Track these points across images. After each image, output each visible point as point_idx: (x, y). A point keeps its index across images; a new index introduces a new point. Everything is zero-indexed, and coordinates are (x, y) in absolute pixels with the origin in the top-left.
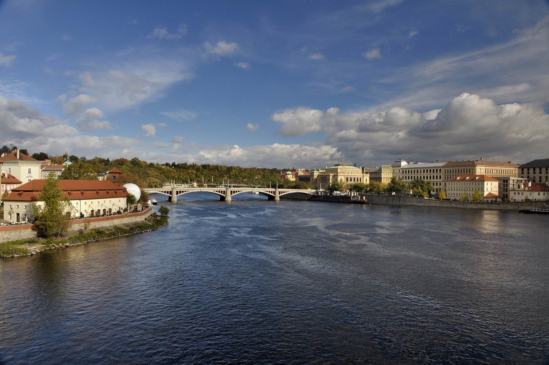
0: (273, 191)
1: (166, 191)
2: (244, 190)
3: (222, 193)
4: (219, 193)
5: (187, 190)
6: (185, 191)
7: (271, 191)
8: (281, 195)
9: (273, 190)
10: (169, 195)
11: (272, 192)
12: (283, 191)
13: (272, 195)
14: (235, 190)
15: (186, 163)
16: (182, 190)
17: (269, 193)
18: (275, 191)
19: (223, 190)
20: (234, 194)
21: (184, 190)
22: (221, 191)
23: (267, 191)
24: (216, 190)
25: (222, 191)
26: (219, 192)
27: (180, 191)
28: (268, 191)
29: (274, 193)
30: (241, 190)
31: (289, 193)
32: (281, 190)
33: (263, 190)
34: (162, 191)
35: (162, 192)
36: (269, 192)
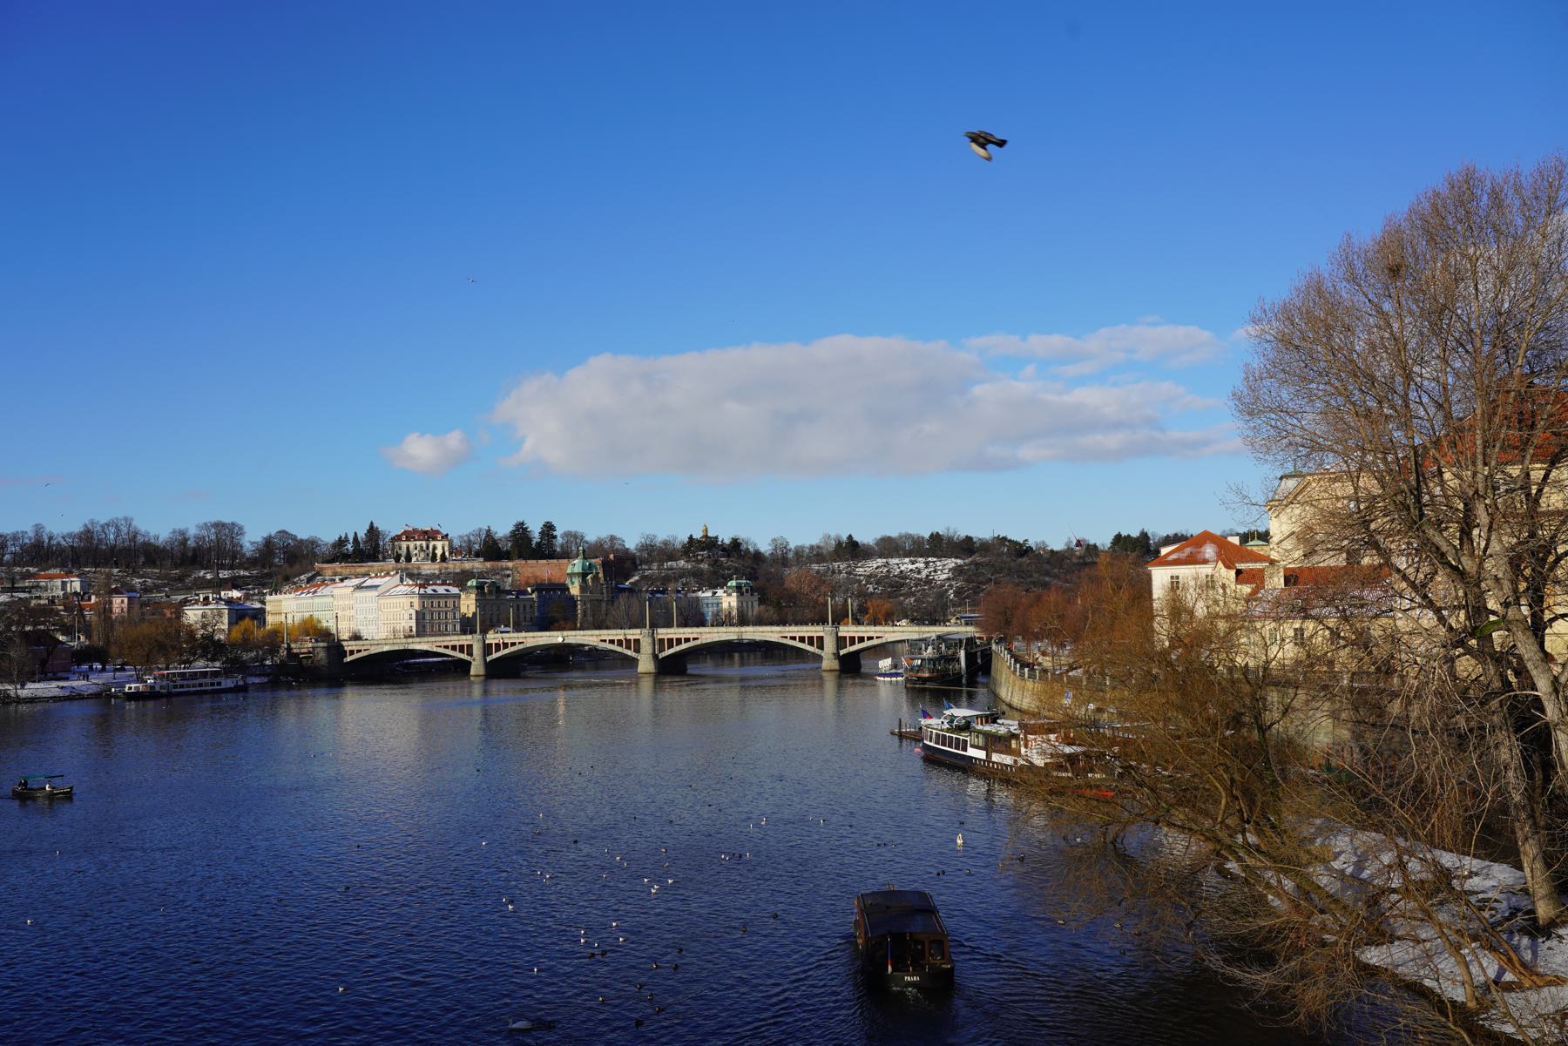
0: (815, 635)
1: (804, 637)
3: (628, 647)
4: (619, 649)
5: (517, 641)
7: (806, 635)
12: (856, 635)
14: (675, 637)
17: (800, 645)
19: (632, 638)
20: (672, 651)
22: (626, 639)
25: (628, 641)
28: (797, 635)
30: (695, 636)
32: (848, 630)
34: (446, 644)
35: (446, 647)
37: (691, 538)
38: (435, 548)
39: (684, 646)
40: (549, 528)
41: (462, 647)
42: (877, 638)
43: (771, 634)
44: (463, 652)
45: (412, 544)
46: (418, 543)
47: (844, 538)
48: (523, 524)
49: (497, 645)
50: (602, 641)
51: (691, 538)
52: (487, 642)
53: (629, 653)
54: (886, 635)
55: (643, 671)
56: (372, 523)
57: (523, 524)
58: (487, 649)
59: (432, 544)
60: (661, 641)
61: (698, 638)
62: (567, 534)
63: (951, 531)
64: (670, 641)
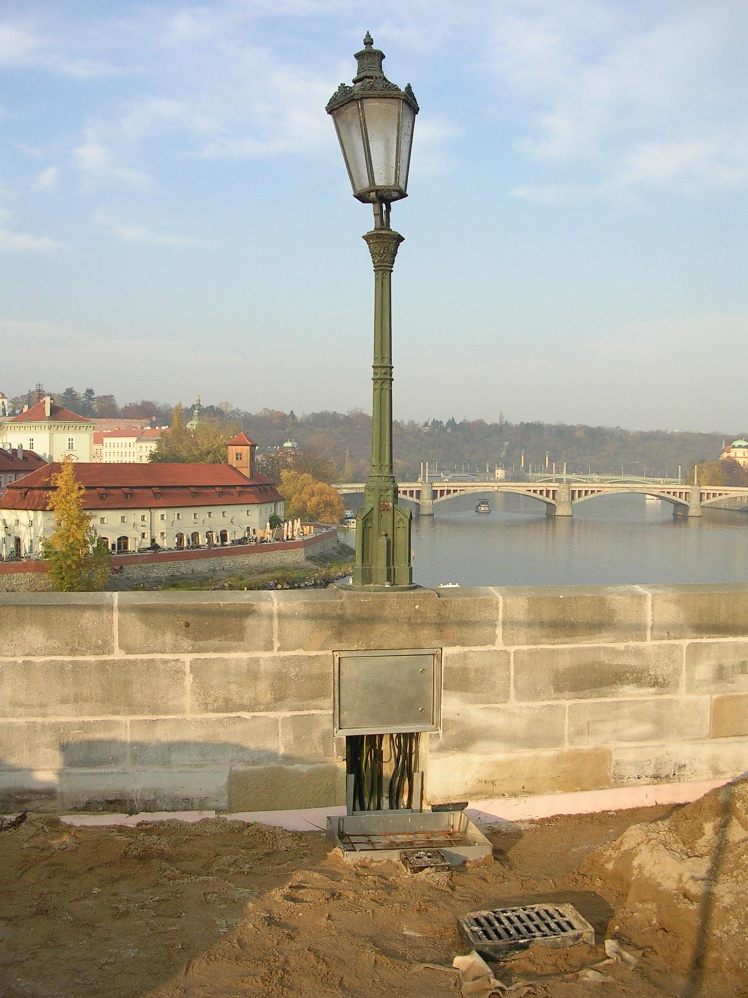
2: (605, 490)
5: (459, 489)
6: (455, 491)
8: (706, 502)
9: (685, 488)
10: (414, 499)
15: (482, 419)
16: (446, 488)
17: (674, 498)
19: (551, 489)
21: (452, 489)
23: (669, 490)
24: (532, 489)
27: (441, 491)
31: (730, 496)
33: (658, 490)
40: (90, 392)
41: (411, 493)
42: (725, 494)
43: (655, 490)
44: (413, 496)
49: (442, 492)
50: (527, 490)
52: (434, 489)
53: (549, 500)
54: (732, 493)
55: (694, 514)
58: (434, 494)
60: (573, 492)
61: (600, 491)
63: (359, 411)
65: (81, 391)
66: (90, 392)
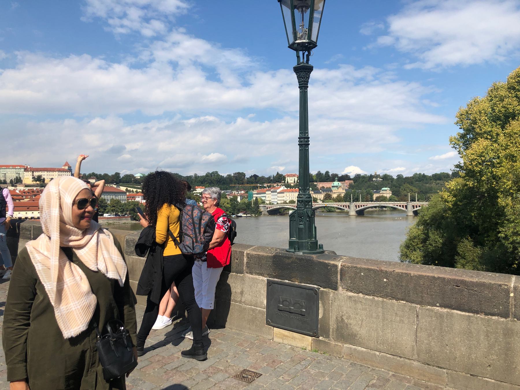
2: (369, 205)
7: (401, 205)
9: (404, 203)
11: (403, 206)
12: (418, 205)
13: (404, 209)
14: (360, 205)
18: (406, 205)
19: (347, 205)
24: (340, 205)
25: (346, 206)
26: (344, 206)
28: (399, 205)
29: (406, 207)
30: (366, 205)
32: (416, 203)
33: (392, 205)
36: (400, 206)
37: (371, 175)
38: (295, 179)
39: (363, 207)
40: (327, 173)
45: (289, 178)
46: (290, 178)
47: (422, 174)
48: (319, 171)
51: (371, 175)
56: (278, 172)
57: (319, 171)
59: (294, 178)
62: (333, 175)
64: (359, 206)
65: (323, 172)
66: (327, 173)
